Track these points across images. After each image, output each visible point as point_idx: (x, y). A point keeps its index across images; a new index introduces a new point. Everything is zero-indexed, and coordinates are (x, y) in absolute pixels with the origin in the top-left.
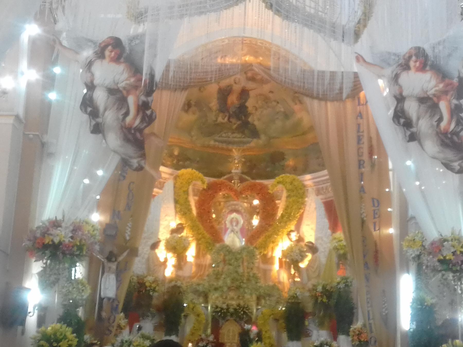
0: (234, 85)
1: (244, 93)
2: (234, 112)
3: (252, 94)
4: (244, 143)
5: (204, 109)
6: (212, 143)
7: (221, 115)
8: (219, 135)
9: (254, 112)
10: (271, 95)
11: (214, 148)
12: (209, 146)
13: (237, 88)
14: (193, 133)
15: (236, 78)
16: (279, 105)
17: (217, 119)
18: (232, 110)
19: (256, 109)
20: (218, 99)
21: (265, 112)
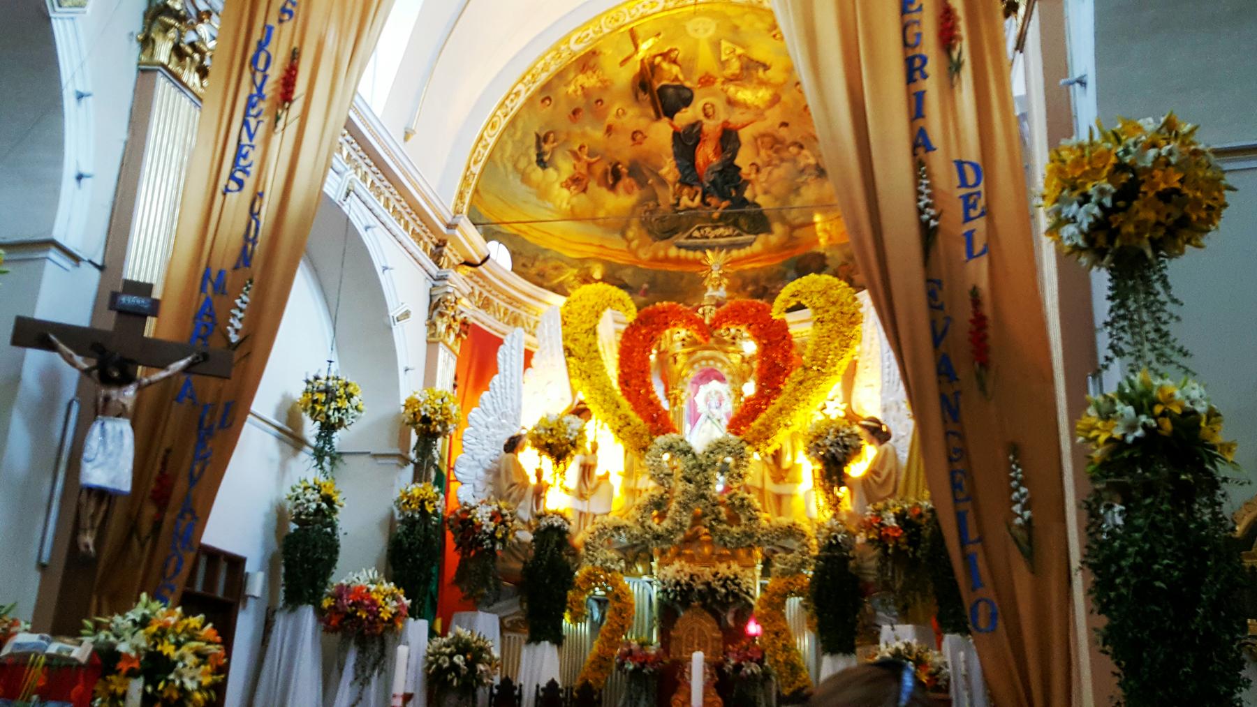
0: (705, 120)
2: (713, 183)
3: (745, 135)
4: (740, 246)
5: (650, 182)
6: (673, 252)
7: (686, 190)
8: (687, 234)
9: (753, 176)
10: (783, 132)
11: (678, 261)
12: (666, 259)
13: (711, 126)
14: (630, 234)
16: (805, 152)
17: (679, 200)
18: (707, 178)
19: (758, 171)
20: (676, 156)
21: (777, 173)
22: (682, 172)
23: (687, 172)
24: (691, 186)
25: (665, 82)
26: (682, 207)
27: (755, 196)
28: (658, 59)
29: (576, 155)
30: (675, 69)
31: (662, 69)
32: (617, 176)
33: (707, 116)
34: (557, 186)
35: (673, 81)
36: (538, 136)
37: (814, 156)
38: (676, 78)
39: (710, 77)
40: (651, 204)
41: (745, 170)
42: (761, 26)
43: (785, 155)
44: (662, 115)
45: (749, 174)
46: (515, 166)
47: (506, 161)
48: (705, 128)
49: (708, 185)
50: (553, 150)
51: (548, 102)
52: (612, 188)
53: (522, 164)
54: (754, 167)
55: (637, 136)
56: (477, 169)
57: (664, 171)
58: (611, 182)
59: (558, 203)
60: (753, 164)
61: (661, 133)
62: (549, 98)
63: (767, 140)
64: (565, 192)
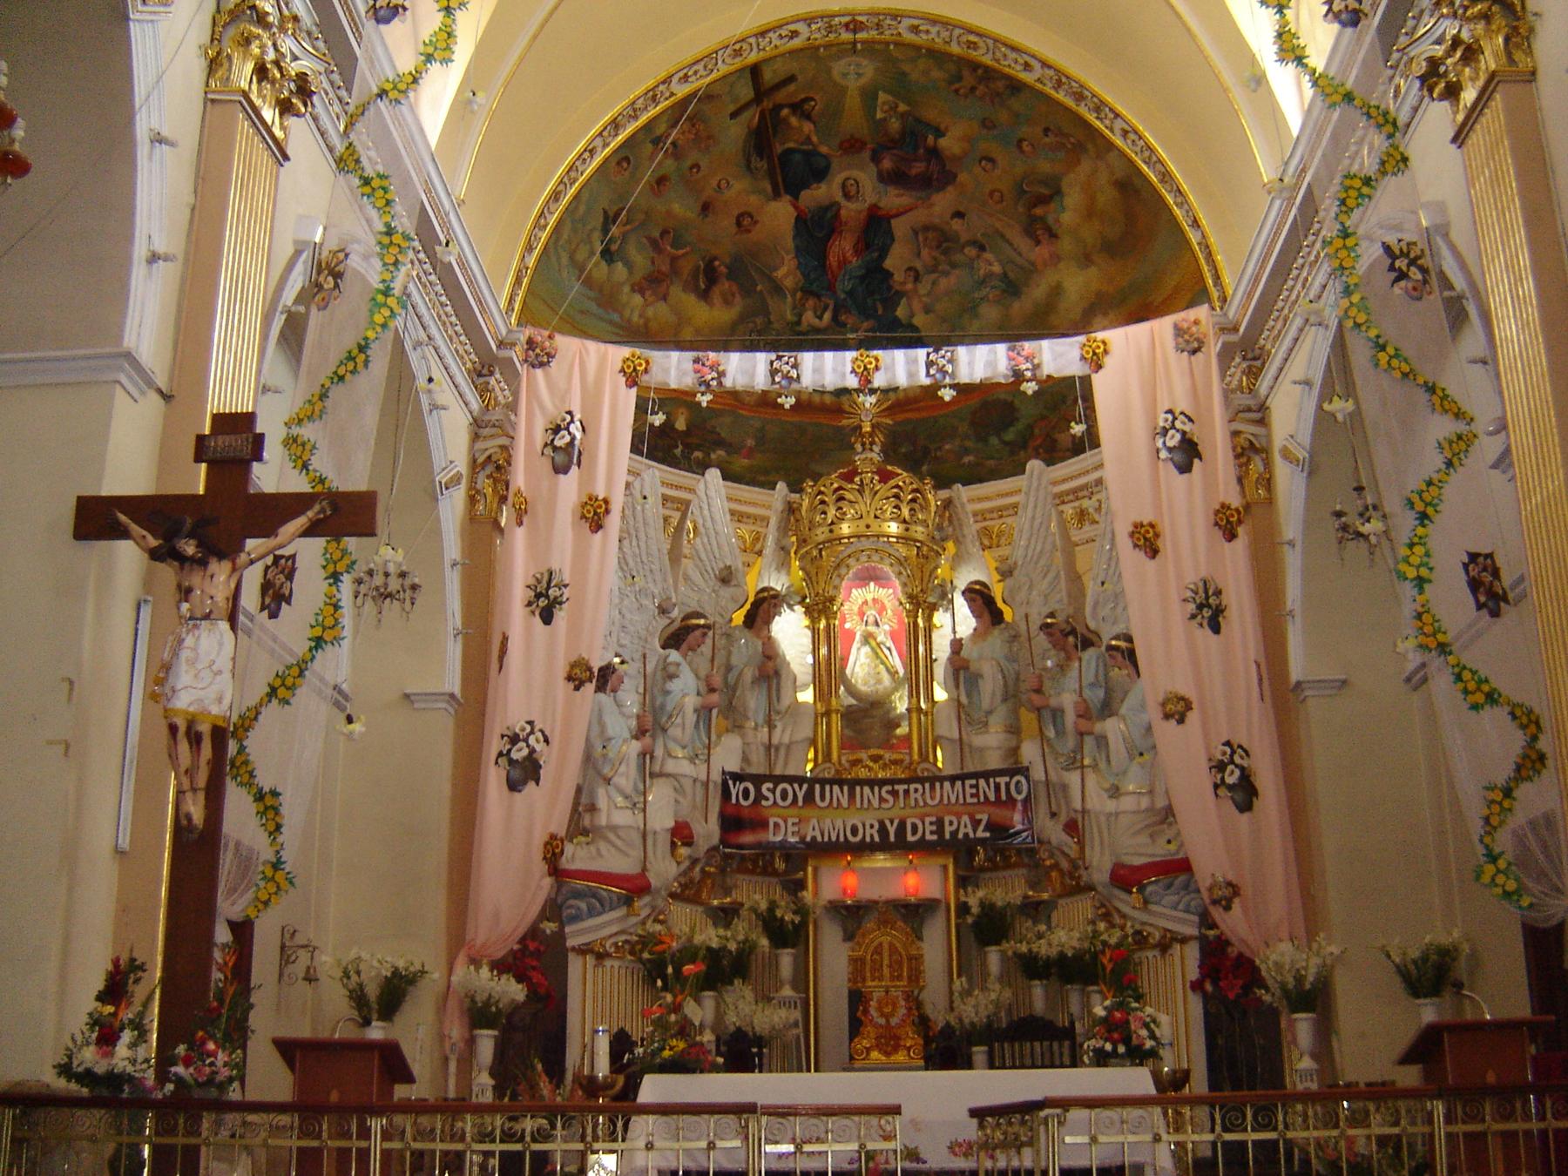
0: (843, 202)
1: (876, 227)
2: (850, 293)
3: (900, 227)
5: (759, 288)
7: (811, 302)
10: (956, 224)
13: (852, 210)
15: (848, 179)
16: (988, 255)
17: (800, 316)
18: (843, 286)
19: (917, 279)
20: (799, 251)
21: (944, 283)
22: (806, 276)
23: (812, 276)
24: (818, 296)
25: (791, 145)
26: (804, 326)
27: (912, 316)
28: (785, 112)
29: (655, 245)
30: (808, 127)
31: (788, 125)
32: (711, 276)
33: (847, 195)
34: (626, 289)
35: (802, 144)
36: (605, 212)
37: (1000, 261)
38: (809, 138)
39: (857, 141)
40: (759, 320)
41: (898, 277)
42: (936, 74)
43: (958, 257)
44: (782, 191)
45: (904, 283)
46: (572, 258)
47: (560, 250)
48: (843, 212)
49: (843, 296)
50: (624, 236)
51: (625, 165)
52: (705, 295)
53: (581, 256)
54: (912, 273)
55: (744, 221)
56: (531, 261)
57: (780, 273)
58: (703, 286)
59: (627, 313)
60: (910, 269)
61: (780, 215)
62: (627, 159)
63: (930, 235)
64: (637, 299)
